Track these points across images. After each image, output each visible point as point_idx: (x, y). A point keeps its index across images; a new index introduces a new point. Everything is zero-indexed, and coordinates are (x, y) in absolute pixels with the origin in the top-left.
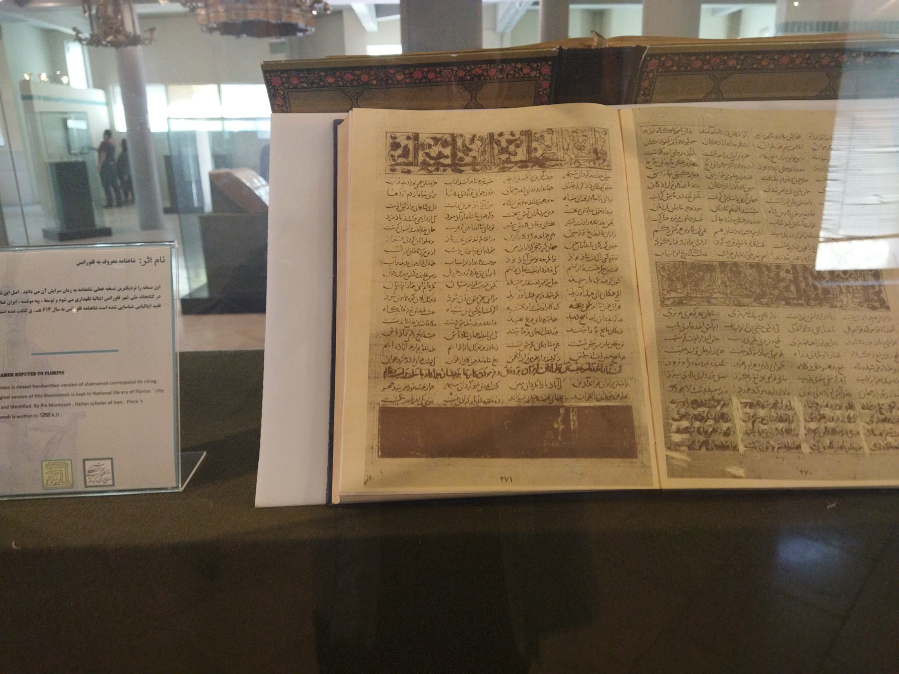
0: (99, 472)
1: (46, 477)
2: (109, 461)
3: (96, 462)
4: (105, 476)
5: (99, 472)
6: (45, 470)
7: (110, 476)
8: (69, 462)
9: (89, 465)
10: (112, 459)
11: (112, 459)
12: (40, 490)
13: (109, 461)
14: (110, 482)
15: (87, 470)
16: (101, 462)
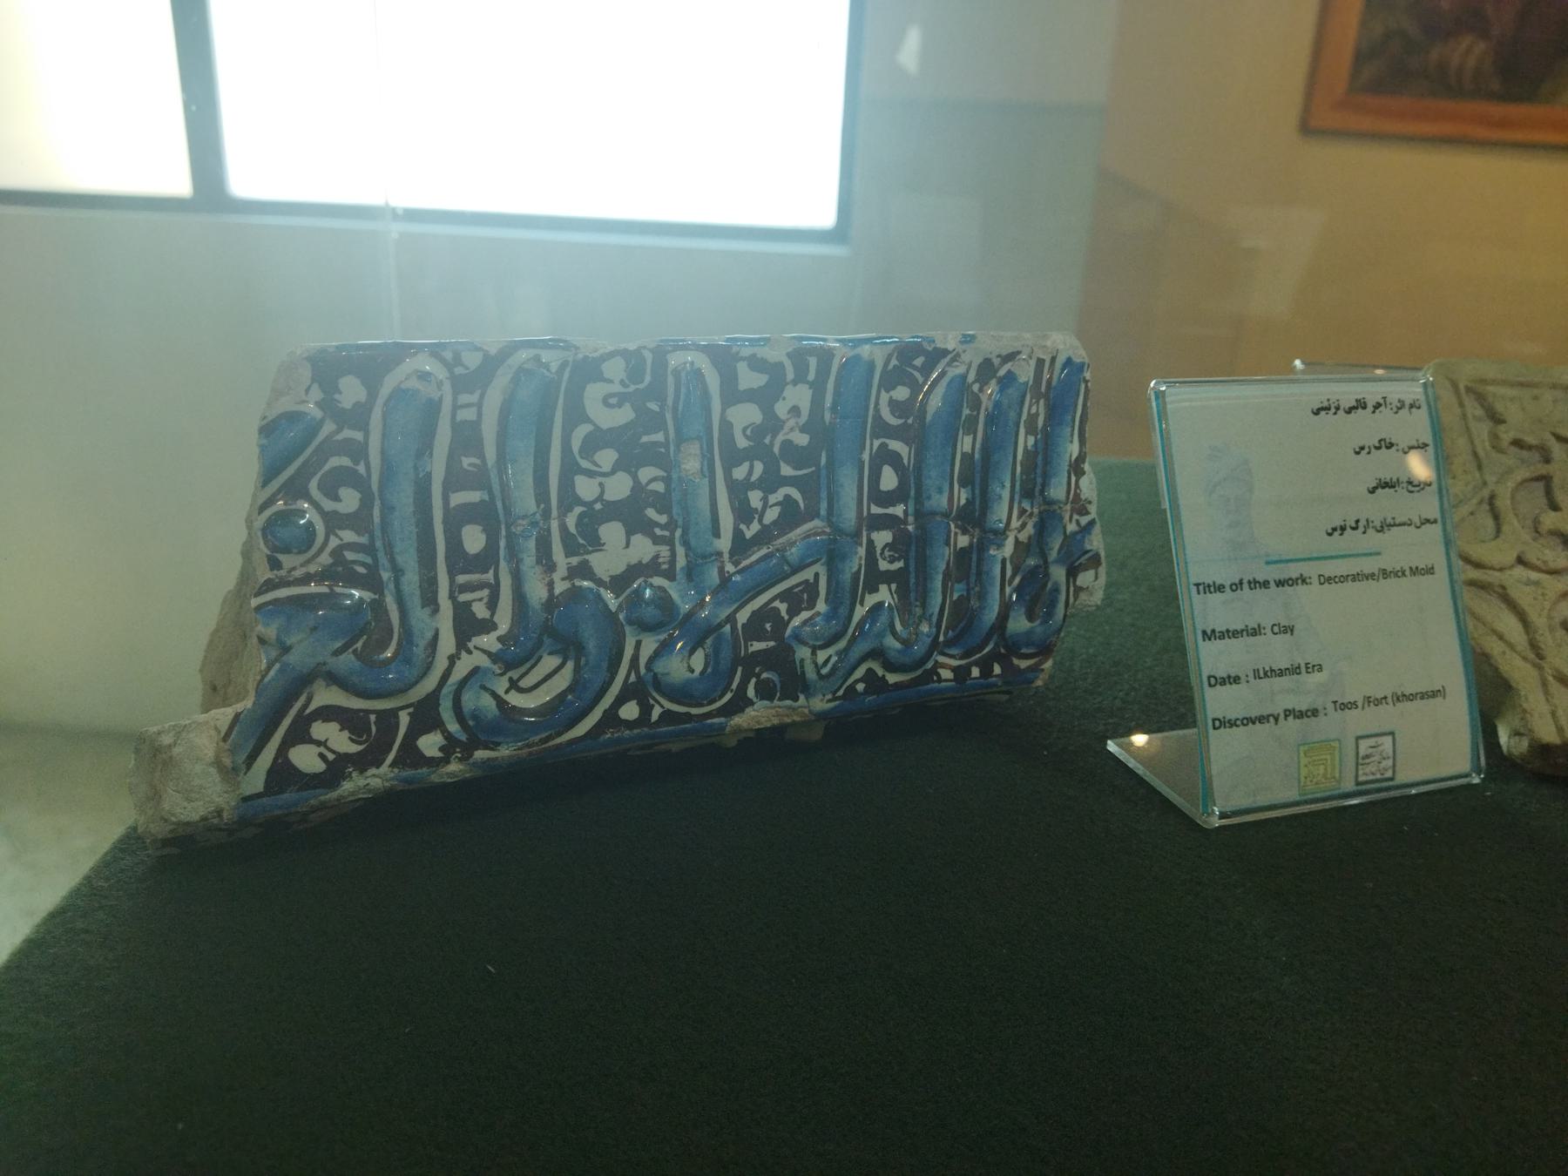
0: (1376, 758)
1: (1304, 772)
2: (1390, 738)
3: (1372, 741)
4: (1384, 764)
5: (1376, 758)
6: (1304, 761)
7: (1390, 762)
8: (1336, 744)
9: (1364, 745)
10: (1392, 734)
11: (1392, 734)
12: (1292, 795)
13: (1390, 738)
14: (1389, 774)
15: (1362, 752)
16: (1380, 740)
